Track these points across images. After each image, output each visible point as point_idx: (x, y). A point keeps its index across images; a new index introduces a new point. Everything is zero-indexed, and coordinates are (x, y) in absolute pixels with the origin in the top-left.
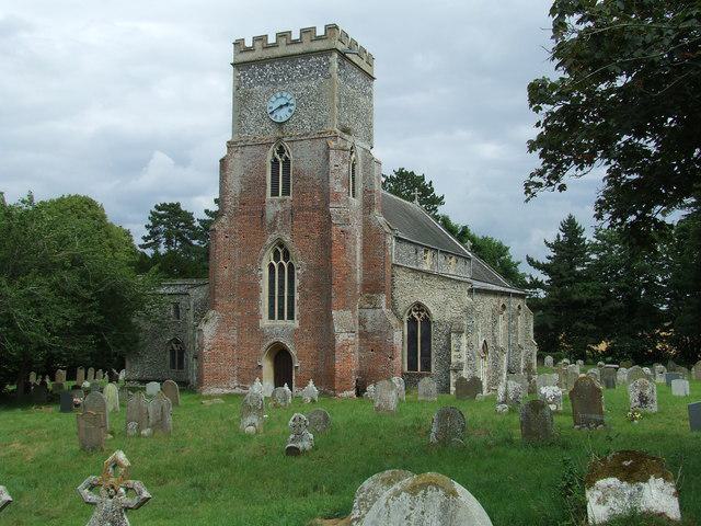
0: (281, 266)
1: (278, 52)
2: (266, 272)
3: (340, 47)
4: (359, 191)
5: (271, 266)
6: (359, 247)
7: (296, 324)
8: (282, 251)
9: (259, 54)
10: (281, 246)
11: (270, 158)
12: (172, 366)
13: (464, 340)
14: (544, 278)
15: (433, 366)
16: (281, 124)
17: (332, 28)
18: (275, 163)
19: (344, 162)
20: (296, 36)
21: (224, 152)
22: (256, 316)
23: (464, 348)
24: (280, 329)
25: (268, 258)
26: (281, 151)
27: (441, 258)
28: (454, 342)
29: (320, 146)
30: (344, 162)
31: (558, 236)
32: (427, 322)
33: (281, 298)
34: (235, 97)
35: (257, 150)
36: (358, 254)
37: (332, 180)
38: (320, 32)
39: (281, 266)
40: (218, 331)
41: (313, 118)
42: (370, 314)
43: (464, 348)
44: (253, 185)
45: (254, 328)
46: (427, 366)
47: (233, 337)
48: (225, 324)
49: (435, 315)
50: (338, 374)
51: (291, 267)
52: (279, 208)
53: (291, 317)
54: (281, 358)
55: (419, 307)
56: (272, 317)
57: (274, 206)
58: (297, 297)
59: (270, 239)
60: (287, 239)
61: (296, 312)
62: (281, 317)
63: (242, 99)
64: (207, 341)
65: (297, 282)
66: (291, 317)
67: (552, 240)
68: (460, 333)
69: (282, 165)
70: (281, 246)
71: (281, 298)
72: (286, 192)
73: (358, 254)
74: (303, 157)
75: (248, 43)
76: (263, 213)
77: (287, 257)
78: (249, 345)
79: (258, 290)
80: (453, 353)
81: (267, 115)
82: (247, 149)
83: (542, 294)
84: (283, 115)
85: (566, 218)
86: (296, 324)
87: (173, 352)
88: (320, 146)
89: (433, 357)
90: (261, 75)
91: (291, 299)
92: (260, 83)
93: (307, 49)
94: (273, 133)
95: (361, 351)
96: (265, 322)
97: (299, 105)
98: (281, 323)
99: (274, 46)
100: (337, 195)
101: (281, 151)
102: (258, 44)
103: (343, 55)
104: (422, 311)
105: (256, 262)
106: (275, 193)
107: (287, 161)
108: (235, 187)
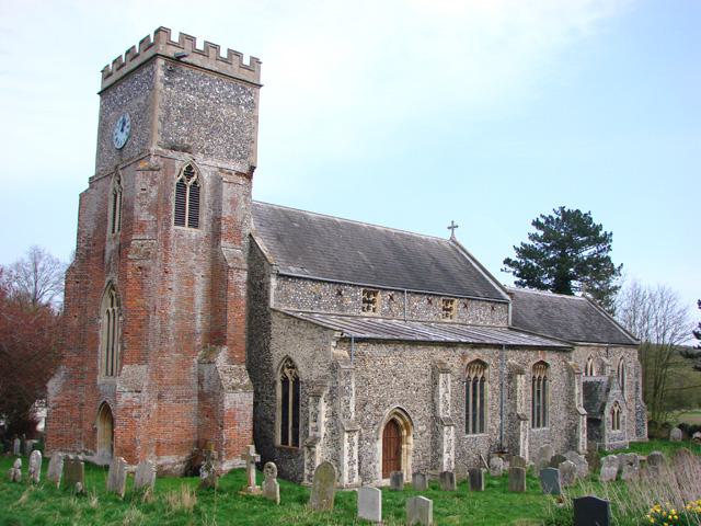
4: (204, 218)
19: (154, 183)
22: (95, 371)
23: (323, 419)
27: (419, 303)
30: (154, 183)
32: (297, 381)
37: (137, 208)
43: (323, 419)
44: (101, 220)
49: (303, 373)
55: (289, 363)
60: (116, 281)
76: (104, 251)
80: (312, 424)
100: (142, 226)
104: (293, 368)
106: (113, 232)
108: (91, 226)
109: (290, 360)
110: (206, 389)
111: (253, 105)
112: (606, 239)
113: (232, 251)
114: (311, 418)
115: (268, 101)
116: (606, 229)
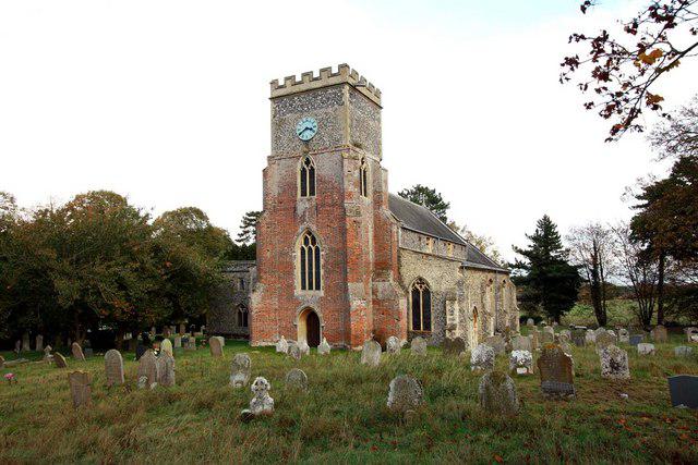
0: (310, 249)
1: (303, 87)
2: (299, 254)
3: (351, 81)
4: (370, 191)
5: (303, 249)
6: (371, 234)
7: (322, 293)
8: (310, 238)
10: (310, 233)
12: (240, 325)
13: (456, 306)
14: (526, 261)
15: (432, 327)
16: (307, 142)
17: (343, 67)
18: (303, 171)
20: (316, 75)
21: (266, 165)
22: (291, 287)
23: (457, 313)
25: (299, 243)
26: (308, 162)
27: (441, 244)
28: (448, 308)
29: (336, 157)
31: (537, 231)
32: (427, 292)
33: (311, 273)
34: (273, 123)
35: (290, 162)
36: (370, 242)
37: (346, 183)
39: (310, 249)
40: (263, 298)
41: (331, 136)
42: (380, 286)
43: (457, 313)
44: (288, 188)
46: (427, 327)
47: (275, 303)
48: (269, 292)
49: (434, 287)
50: (353, 333)
51: (317, 250)
53: (318, 288)
54: (312, 319)
55: (421, 281)
56: (304, 288)
57: (303, 205)
59: (301, 228)
60: (314, 228)
62: (311, 288)
63: (278, 124)
65: (322, 262)
67: (532, 233)
68: (453, 300)
69: (309, 174)
70: (310, 233)
71: (311, 273)
72: (312, 193)
73: (370, 242)
74: (324, 166)
75: (281, 83)
77: (314, 243)
78: (287, 309)
79: (291, 266)
80: (448, 317)
81: (295, 136)
82: (283, 161)
83: (524, 273)
84: (308, 135)
85: (541, 218)
86: (322, 293)
87: (240, 313)
88: (336, 157)
89: (432, 318)
90: (291, 105)
91: (318, 273)
92: (291, 112)
93: (325, 84)
94: (302, 148)
95: (374, 314)
96: (298, 291)
97: (320, 127)
98: (311, 292)
99: (300, 83)
101: (308, 162)
102: (288, 82)
103: (353, 88)
105: (291, 246)
106: (304, 194)
107: (312, 170)
108: (275, 191)
109: (421, 279)
110: (380, 296)
111: (379, 120)
112: (444, 207)
113: (386, 212)
114: (448, 313)
115: (385, 114)
116: (445, 201)
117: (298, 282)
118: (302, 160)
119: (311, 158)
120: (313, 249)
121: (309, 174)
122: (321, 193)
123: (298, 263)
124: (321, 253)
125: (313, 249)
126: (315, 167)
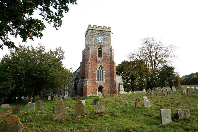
1: (99, 29)
2: (97, 71)
7: (104, 82)
9: (95, 28)
11: (98, 49)
22: (95, 80)
24: (101, 83)
26: (100, 48)
35: (95, 47)
38: (108, 28)
41: (107, 43)
45: (95, 83)
52: (100, 59)
53: (103, 80)
56: (98, 80)
58: (104, 76)
59: (99, 65)
60: (102, 65)
61: (104, 79)
62: (100, 80)
64: (87, 85)
65: (104, 74)
66: (103, 80)
72: (101, 56)
74: (105, 50)
79: (95, 75)
84: (100, 41)
91: (103, 77)
94: (98, 44)
96: (97, 82)
101: (100, 48)
102: (94, 26)
107: (101, 50)
114: (121, 87)
117: (97, 79)
118: (99, 47)
119: (102, 47)
120: (101, 70)
121: (100, 53)
122: (104, 56)
123: (97, 74)
124: (104, 72)
125: (101, 70)
126: (103, 50)
